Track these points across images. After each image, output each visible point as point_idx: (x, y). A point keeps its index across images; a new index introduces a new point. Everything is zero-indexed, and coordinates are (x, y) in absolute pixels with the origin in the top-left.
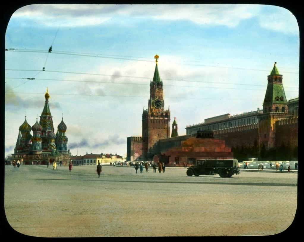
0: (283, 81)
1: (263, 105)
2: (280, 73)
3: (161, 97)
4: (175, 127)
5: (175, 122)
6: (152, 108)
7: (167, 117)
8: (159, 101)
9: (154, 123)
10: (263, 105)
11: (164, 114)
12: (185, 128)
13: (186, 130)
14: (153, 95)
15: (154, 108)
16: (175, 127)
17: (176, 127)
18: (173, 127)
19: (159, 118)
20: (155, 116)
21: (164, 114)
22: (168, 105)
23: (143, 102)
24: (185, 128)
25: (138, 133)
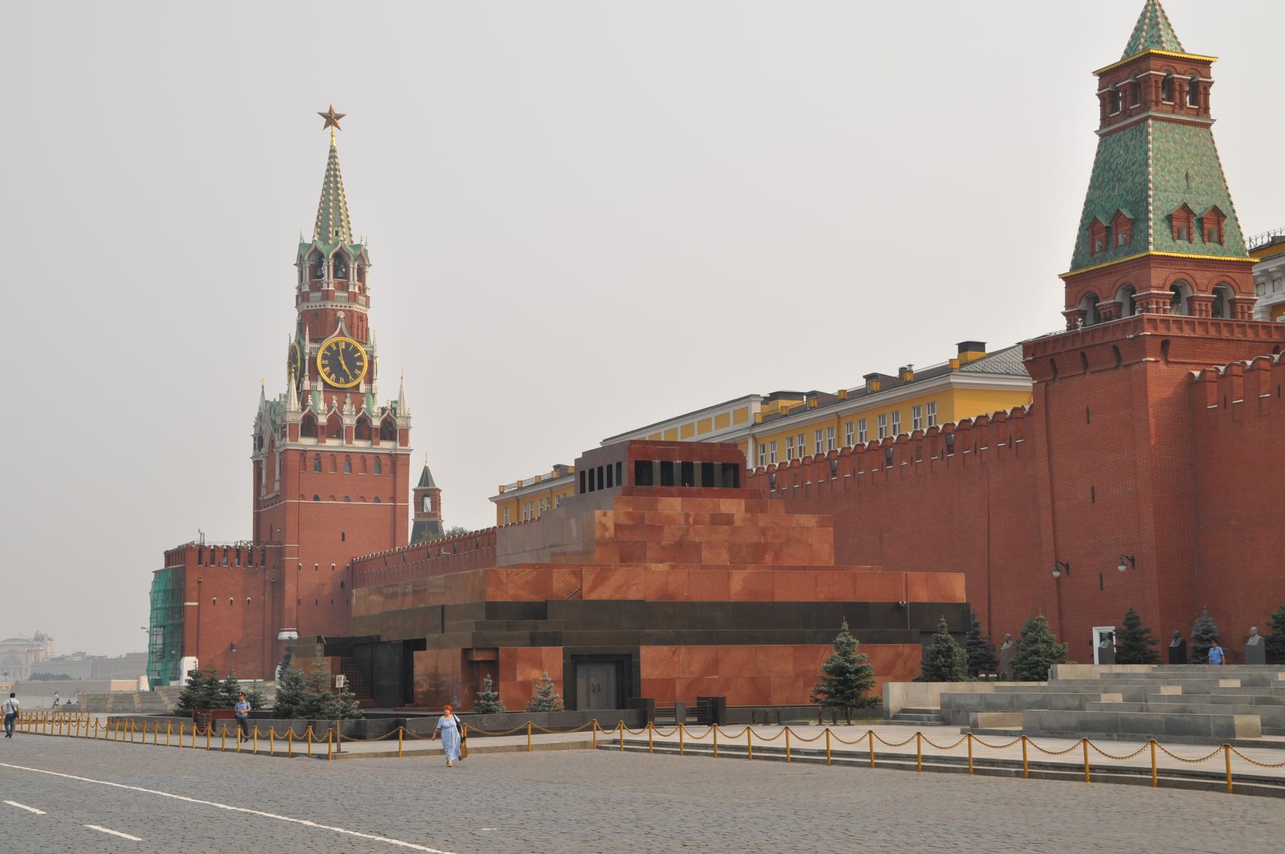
0: (1217, 100)
1: (1065, 278)
2: (1192, 48)
3: (358, 326)
4: (428, 501)
5: (426, 477)
6: (307, 384)
7: (393, 438)
8: (351, 354)
9: (318, 467)
10: (1065, 278)
11: (376, 423)
12: (491, 499)
13: (495, 505)
14: (314, 322)
15: (320, 386)
16: (428, 501)
17: (436, 504)
18: (419, 504)
19: (349, 442)
20: (328, 432)
21: (376, 423)
22: (397, 373)
23: (260, 361)
24: (491, 499)
25: (233, 526)
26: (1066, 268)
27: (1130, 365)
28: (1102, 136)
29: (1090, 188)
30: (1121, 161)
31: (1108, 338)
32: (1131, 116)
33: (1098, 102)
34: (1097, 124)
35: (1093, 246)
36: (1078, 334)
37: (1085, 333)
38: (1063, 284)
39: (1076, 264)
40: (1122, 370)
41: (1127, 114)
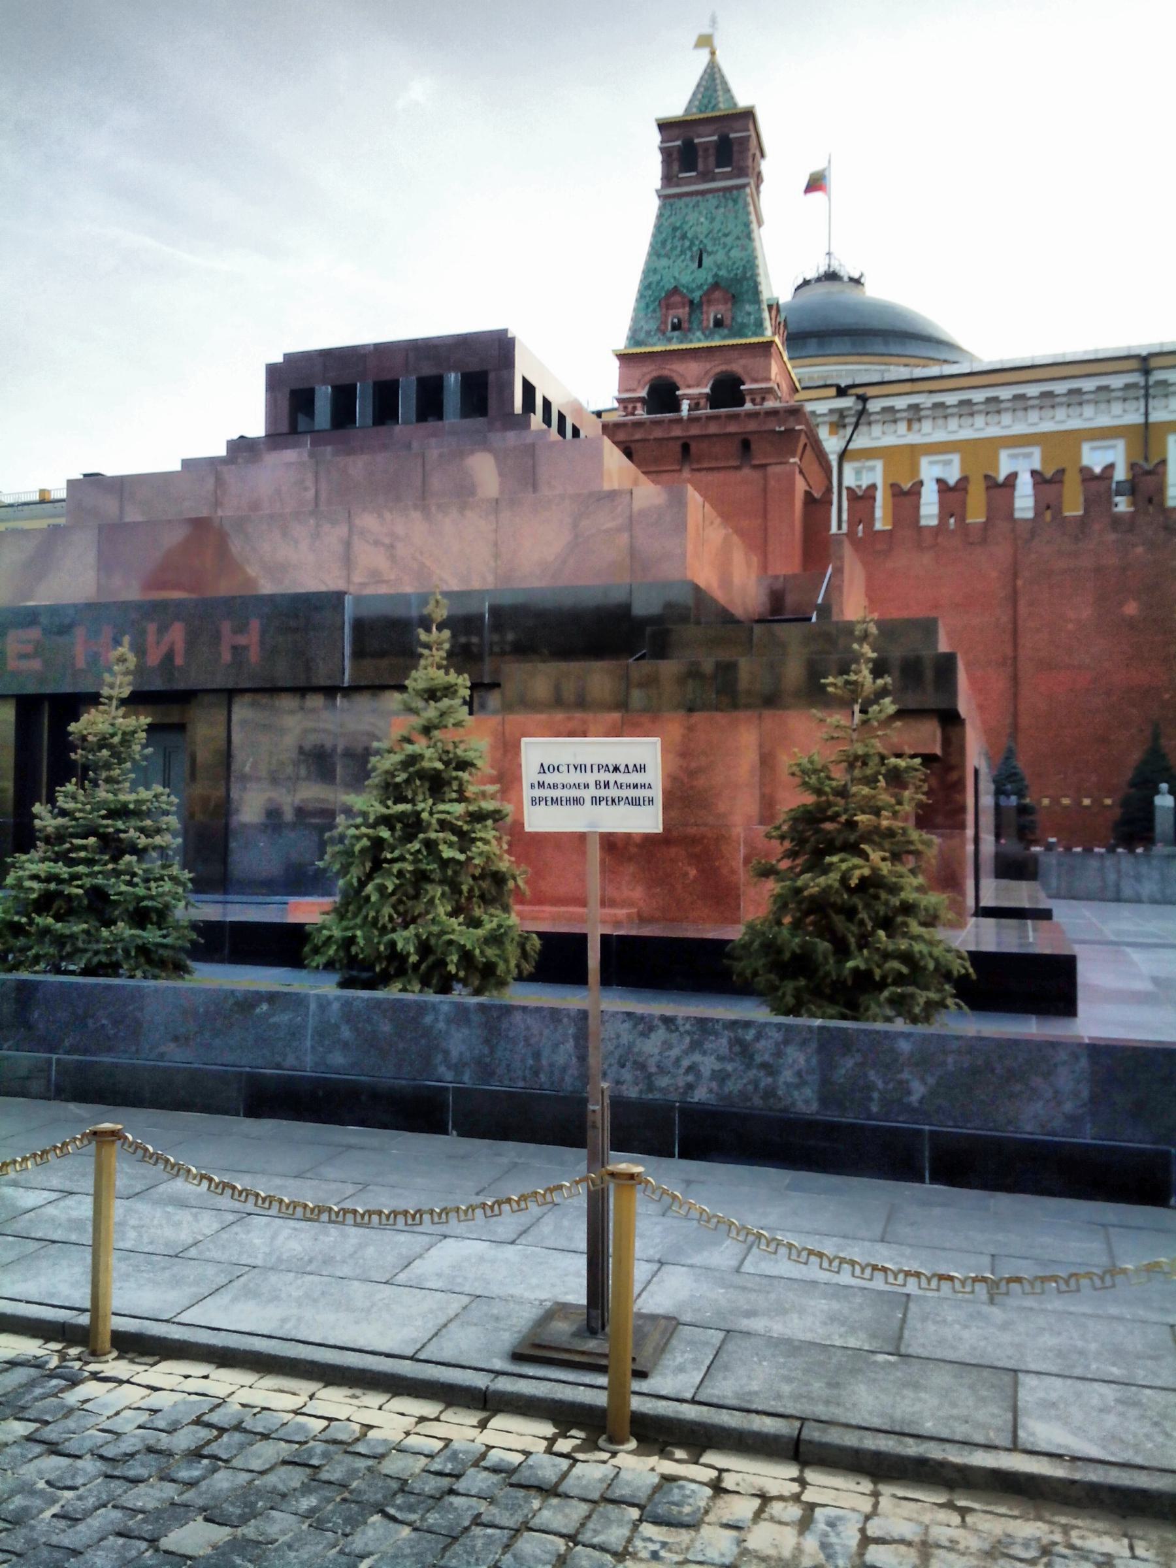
26: (620, 342)
27: (763, 466)
28: (664, 198)
29: (650, 255)
30: (702, 230)
31: (732, 428)
32: (713, 180)
33: (658, 158)
34: (657, 183)
35: (665, 323)
36: (680, 421)
37: (692, 420)
38: (616, 363)
39: (634, 339)
40: (746, 472)
41: (707, 176)
